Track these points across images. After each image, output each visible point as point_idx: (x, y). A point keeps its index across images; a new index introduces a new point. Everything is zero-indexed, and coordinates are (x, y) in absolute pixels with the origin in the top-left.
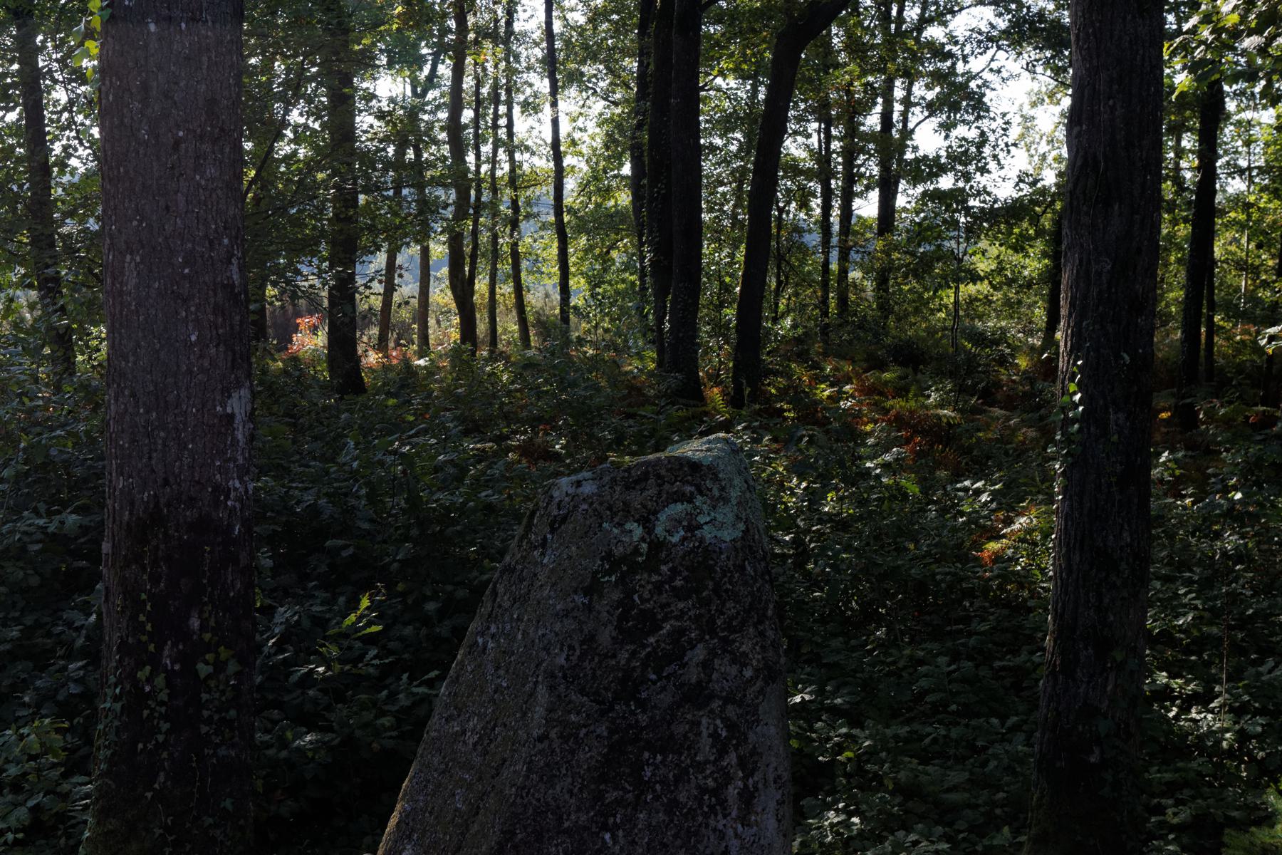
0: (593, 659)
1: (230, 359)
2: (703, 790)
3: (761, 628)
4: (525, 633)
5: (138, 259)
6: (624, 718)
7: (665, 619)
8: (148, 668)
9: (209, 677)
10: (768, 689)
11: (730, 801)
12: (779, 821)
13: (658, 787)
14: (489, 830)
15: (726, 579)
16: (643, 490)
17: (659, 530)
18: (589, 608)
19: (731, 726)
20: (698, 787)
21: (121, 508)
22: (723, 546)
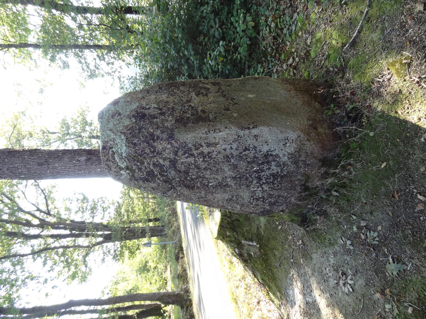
2: (204, 161)
6: (177, 183)
7: (150, 168)
15: (138, 151)
19: (185, 153)
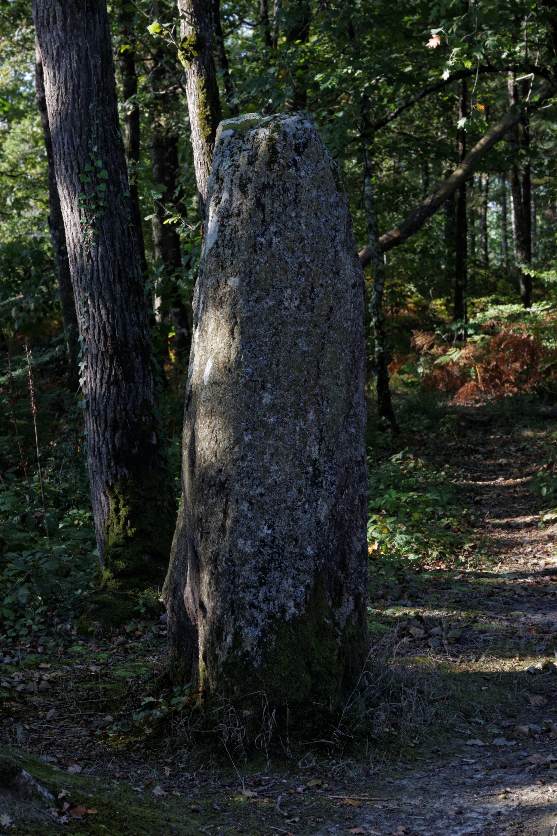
14: (340, 354)
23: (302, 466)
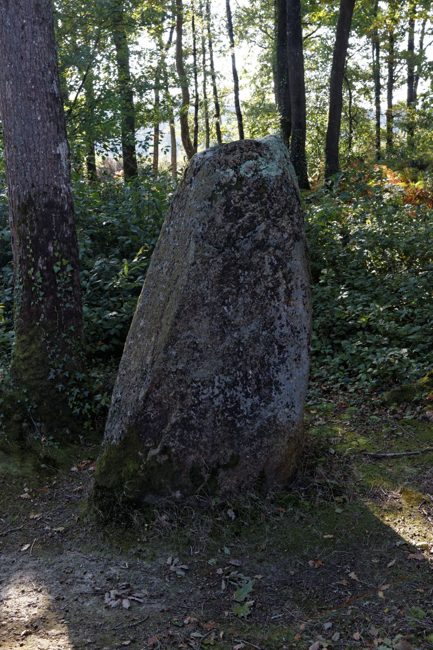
0: (214, 229)
1: (56, 128)
2: (268, 288)
3: (291, 216)
4: (185, 221)
5: (11, 83)
6: (230, 255)
7: (246, 212)
8: (32, 269)
9: (59, 272)
10: (296, 244)
11: (281, 295)
12: (304, 305)
13: (247, 286)
15: (273, 193)
16: (233, 155)
17: (242, 172)
18: (211, 206)
19: (278, 259)
20: (265, 287)
21: (15, 200)
22: (271, 178)
23: (142, 366)
